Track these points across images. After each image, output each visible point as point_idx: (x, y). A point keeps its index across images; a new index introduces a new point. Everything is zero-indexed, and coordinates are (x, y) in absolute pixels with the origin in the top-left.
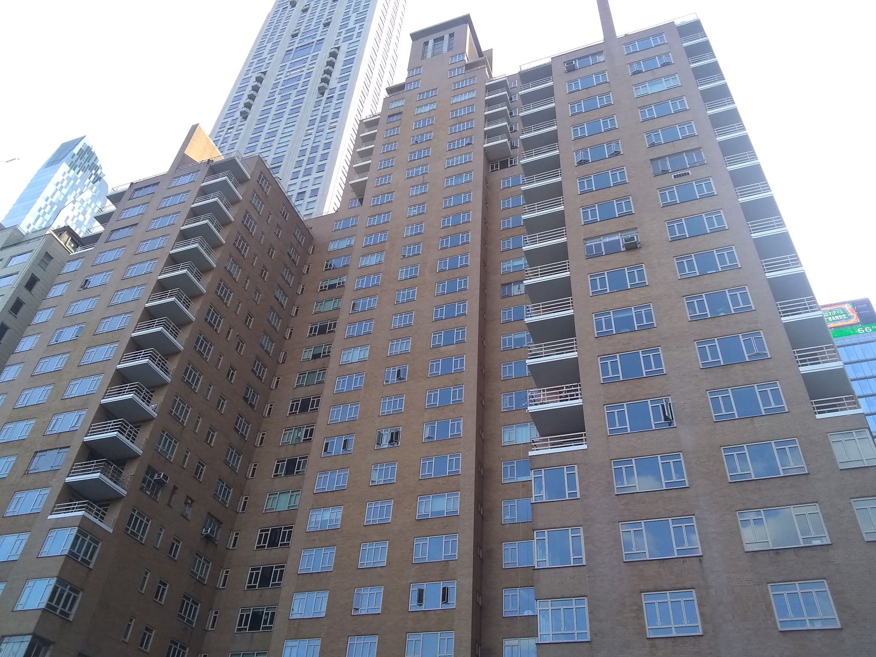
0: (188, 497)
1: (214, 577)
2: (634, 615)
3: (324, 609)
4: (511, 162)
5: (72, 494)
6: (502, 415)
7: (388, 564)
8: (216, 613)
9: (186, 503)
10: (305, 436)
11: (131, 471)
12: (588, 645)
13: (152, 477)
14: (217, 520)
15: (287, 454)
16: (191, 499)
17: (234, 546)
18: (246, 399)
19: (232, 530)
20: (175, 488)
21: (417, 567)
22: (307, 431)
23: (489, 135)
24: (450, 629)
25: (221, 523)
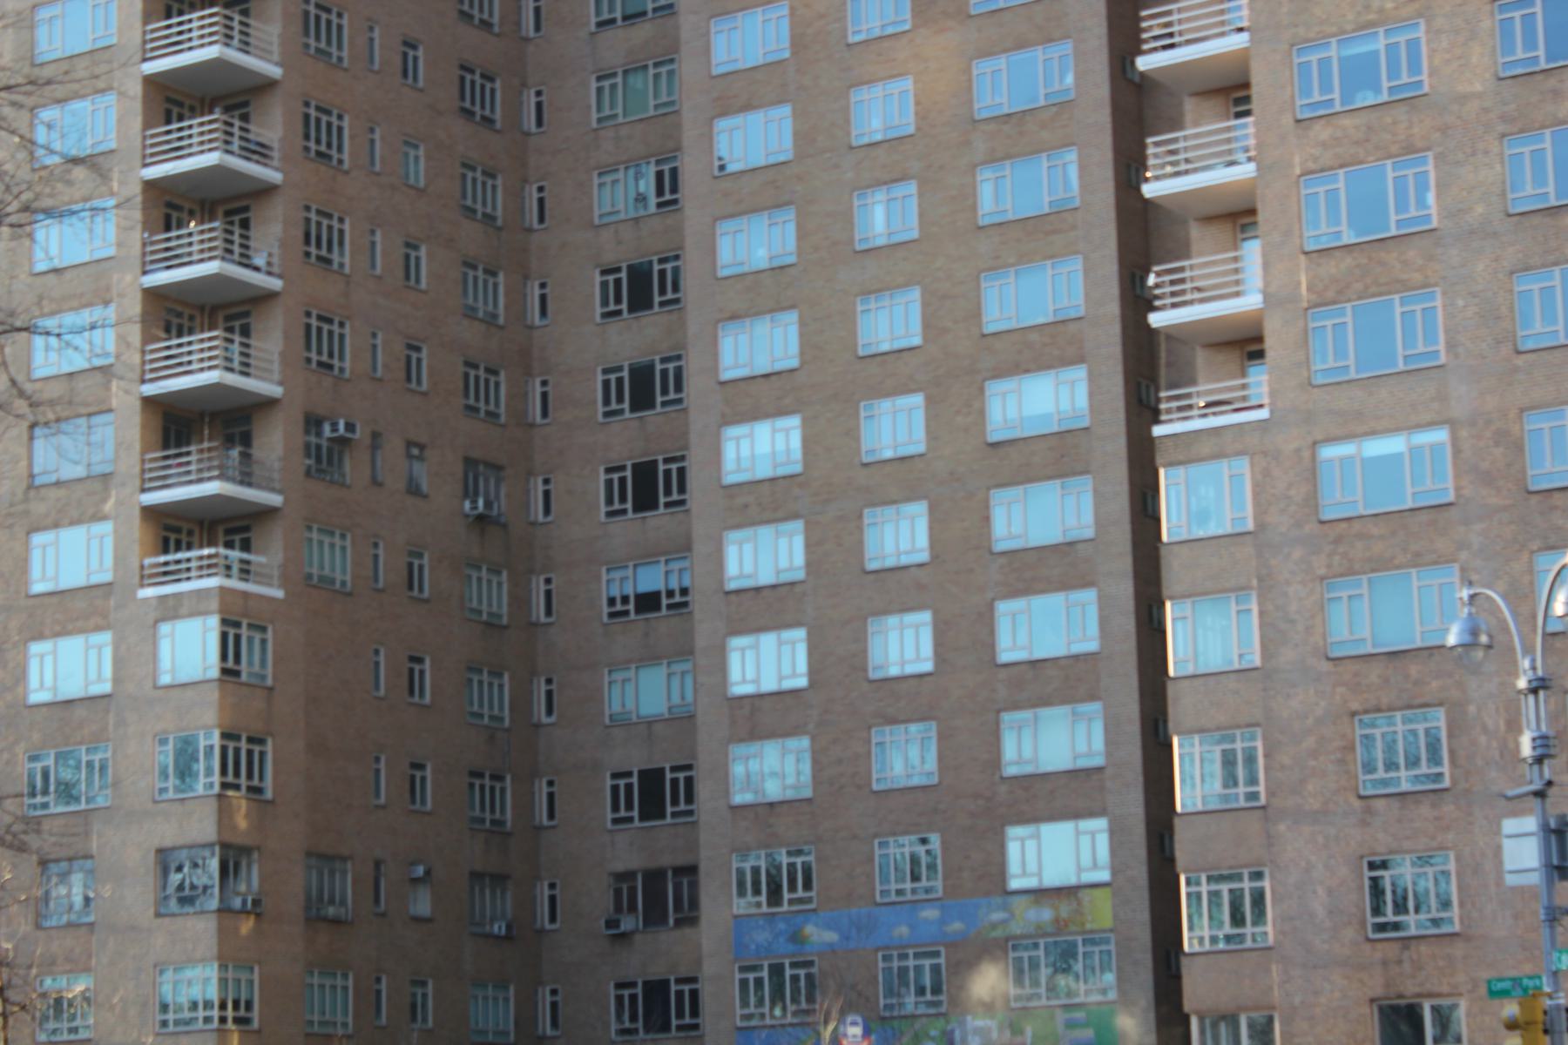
0: (410, 444)
1: (520, 601)
2: (1339, 755)
3: (802, 665)
5: (174, 529)
7: (935, 556)
8: (549, 681)
9: (410, 456)
10: (660, 191)
11: (274, 442)
12: (1259, 813)
13: (319, 434)
14: (488, 465)
15: (623, 253)
16: (417, 445)
17: (547, 511)
18: (468, 113)
19: (530, 473)
20: (375, 435)
21: (1002, 560)
22: (659, 176)
24: (1092, 697)
25: (498, 468)
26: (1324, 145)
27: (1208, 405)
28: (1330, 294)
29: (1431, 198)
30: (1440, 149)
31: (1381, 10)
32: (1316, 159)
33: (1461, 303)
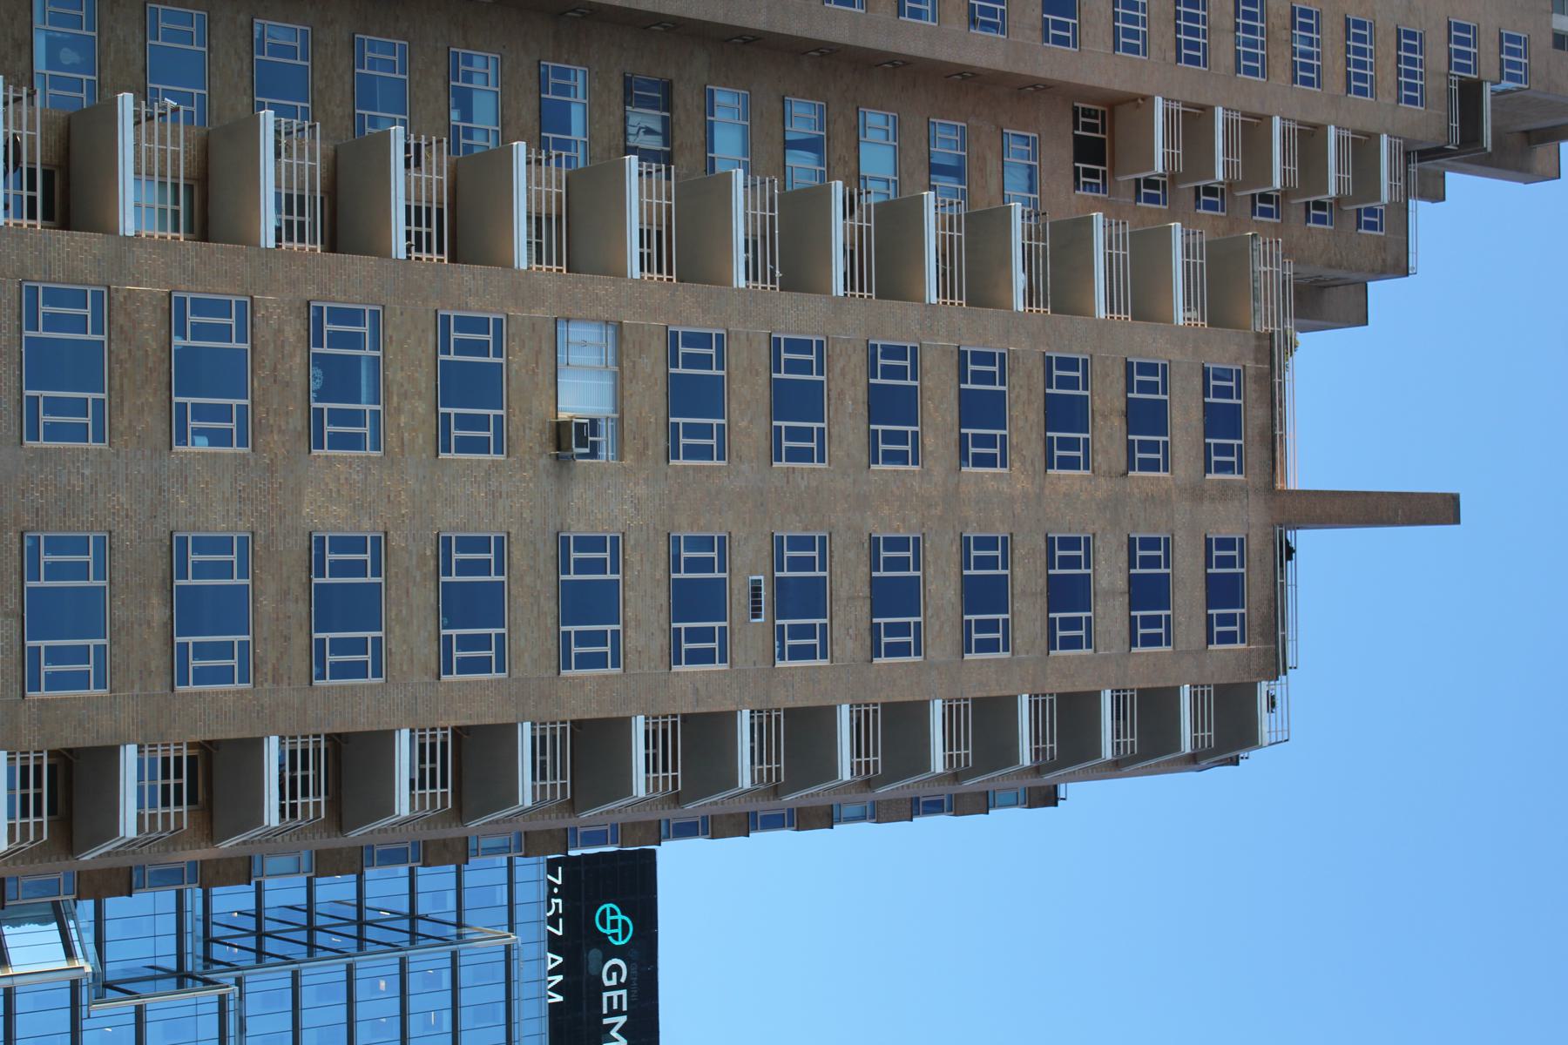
4: (1087, 173)
6: (243, 18)
23: (1193, 122)
26: (280, 331)
27: (17, 145)
28: (121, 319)
29: (202, 445)
30: (252, 463)
31: (399, 410)
32: (266, 319)
33: (87, 472)
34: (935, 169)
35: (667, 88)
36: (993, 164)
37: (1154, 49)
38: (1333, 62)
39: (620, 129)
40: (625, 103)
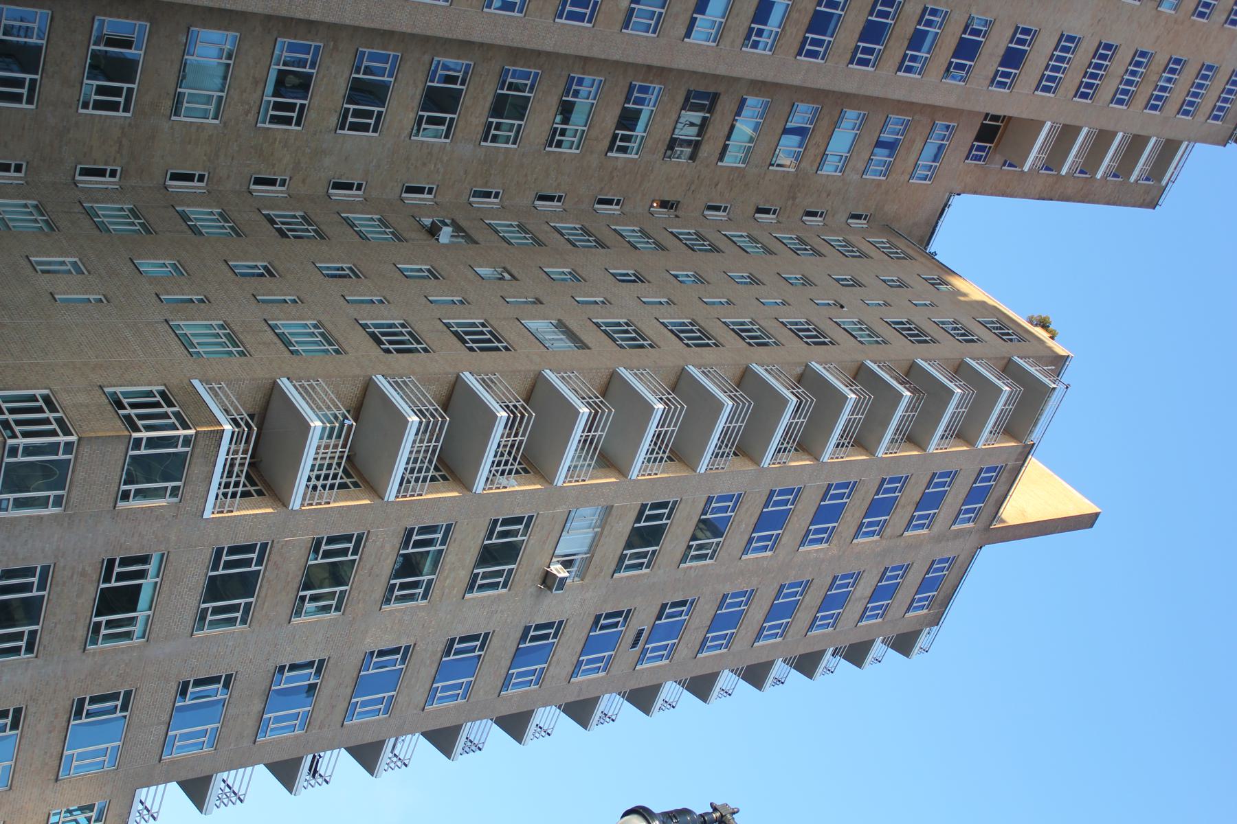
34: (879, 144)
35: (714, 98)
36: (918, 145)
37: (1061, 91)
38: (1178, 95)
39: (671, 128)
40: (683, 108)
